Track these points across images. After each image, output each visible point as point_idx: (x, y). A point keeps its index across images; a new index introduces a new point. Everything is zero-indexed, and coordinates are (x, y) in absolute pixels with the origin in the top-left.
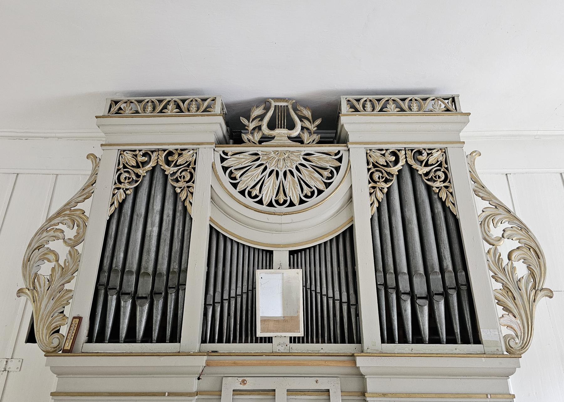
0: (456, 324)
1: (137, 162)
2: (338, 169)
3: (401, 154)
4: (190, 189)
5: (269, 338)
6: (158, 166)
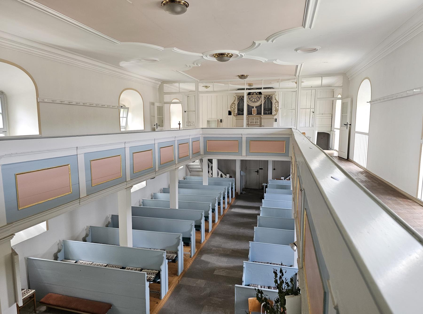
2: (261, 98)
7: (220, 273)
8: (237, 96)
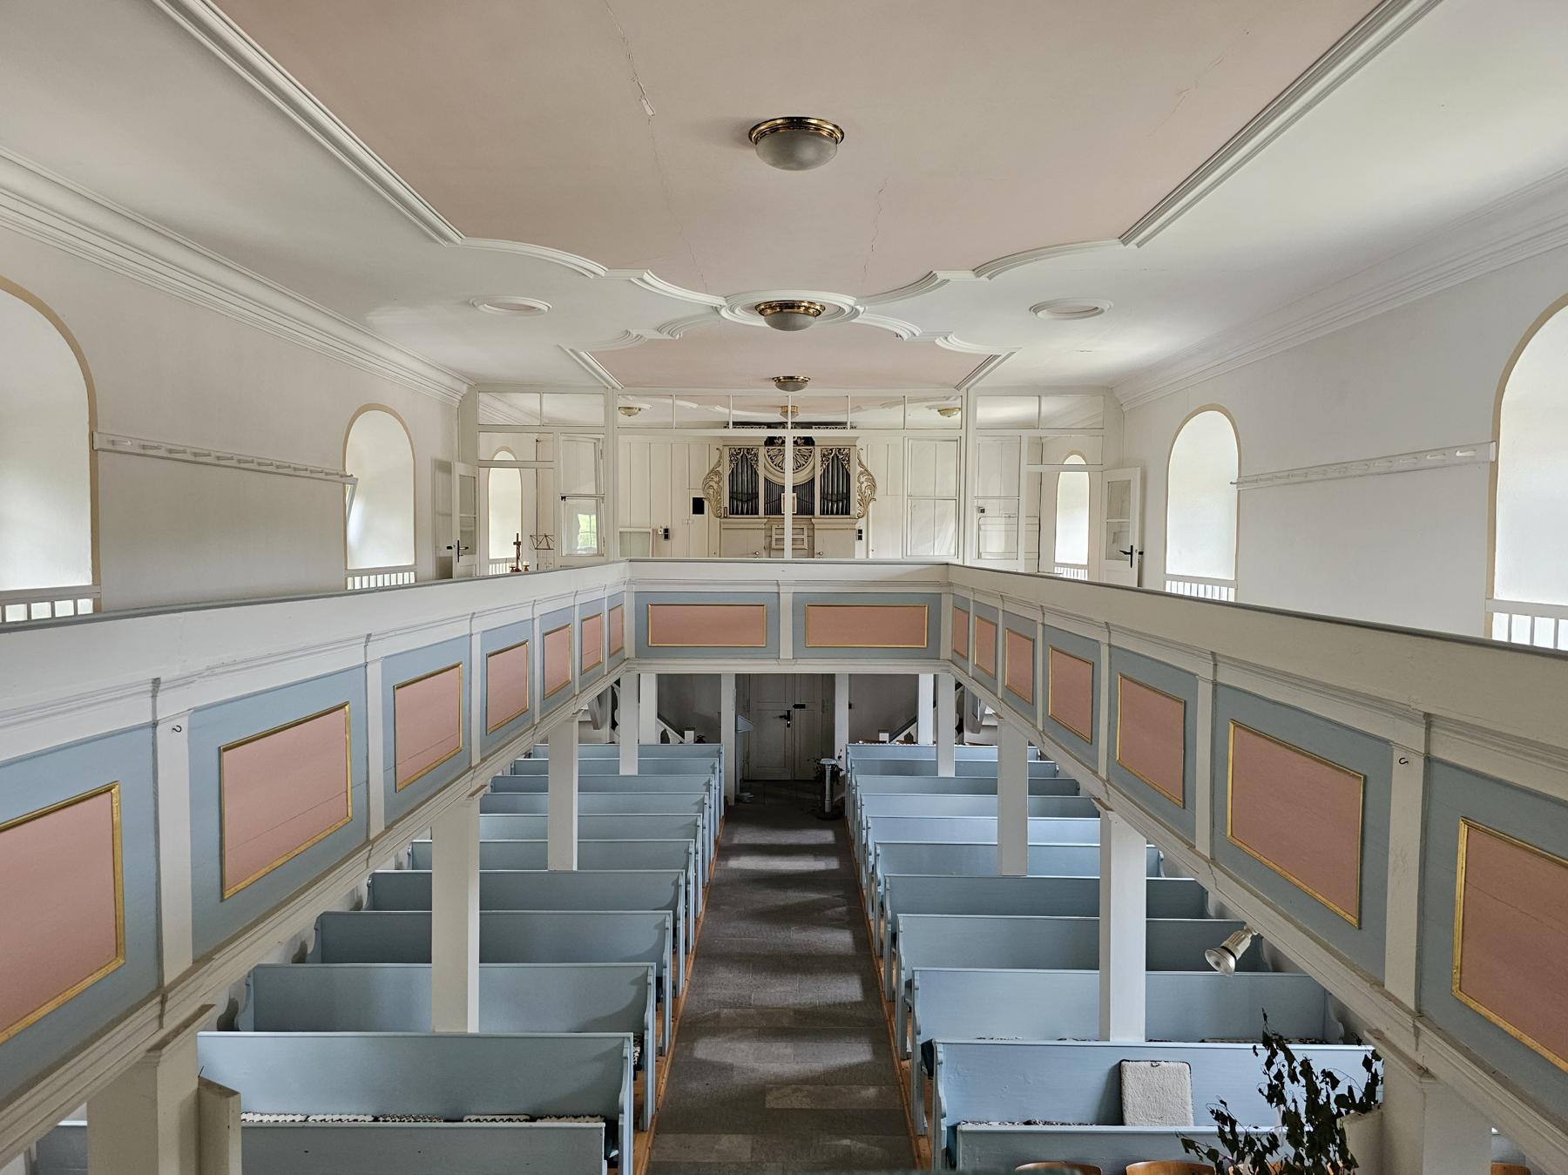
7: (789, 1102)
8: (727, 448)
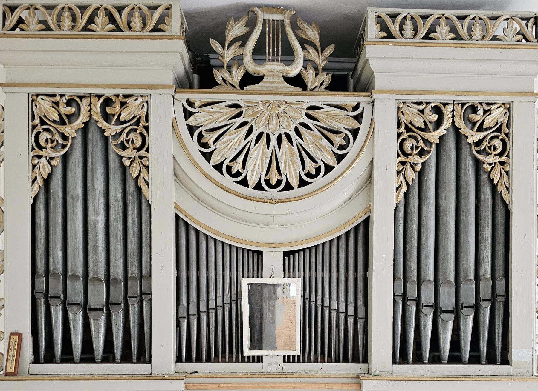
0: (483, 341)
1: (60, 115)
2: (355, 132)
3: (447, 110)
4: (144, 161)
5: (258, 357)
6: (92, 121)
